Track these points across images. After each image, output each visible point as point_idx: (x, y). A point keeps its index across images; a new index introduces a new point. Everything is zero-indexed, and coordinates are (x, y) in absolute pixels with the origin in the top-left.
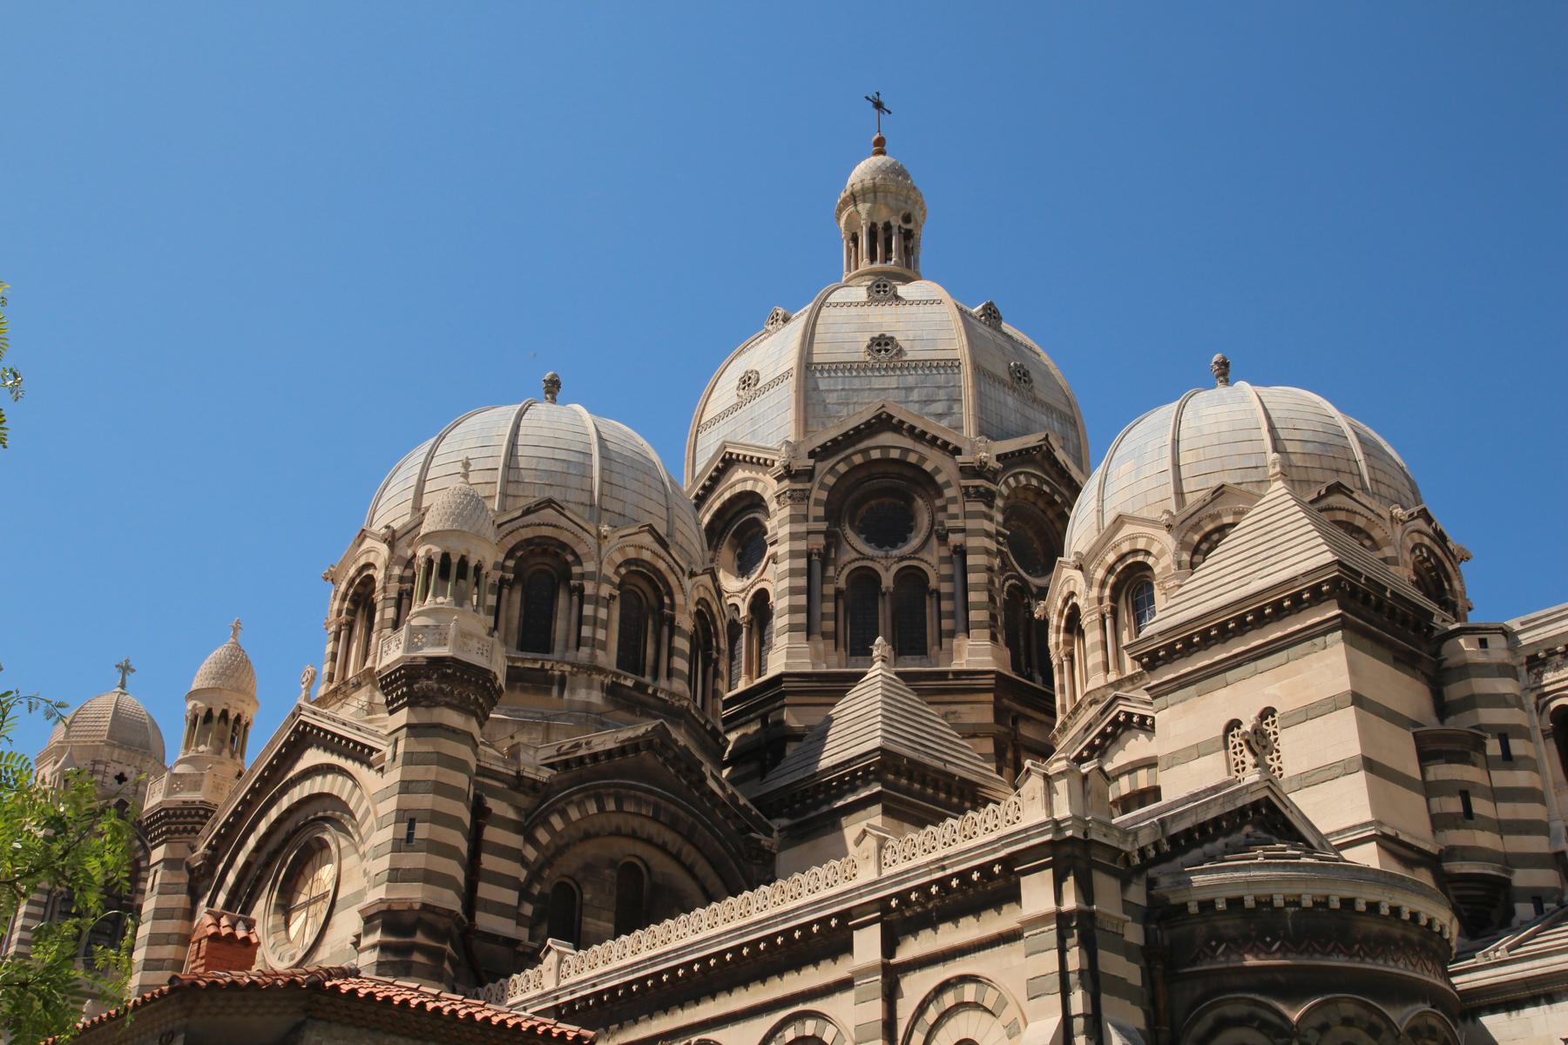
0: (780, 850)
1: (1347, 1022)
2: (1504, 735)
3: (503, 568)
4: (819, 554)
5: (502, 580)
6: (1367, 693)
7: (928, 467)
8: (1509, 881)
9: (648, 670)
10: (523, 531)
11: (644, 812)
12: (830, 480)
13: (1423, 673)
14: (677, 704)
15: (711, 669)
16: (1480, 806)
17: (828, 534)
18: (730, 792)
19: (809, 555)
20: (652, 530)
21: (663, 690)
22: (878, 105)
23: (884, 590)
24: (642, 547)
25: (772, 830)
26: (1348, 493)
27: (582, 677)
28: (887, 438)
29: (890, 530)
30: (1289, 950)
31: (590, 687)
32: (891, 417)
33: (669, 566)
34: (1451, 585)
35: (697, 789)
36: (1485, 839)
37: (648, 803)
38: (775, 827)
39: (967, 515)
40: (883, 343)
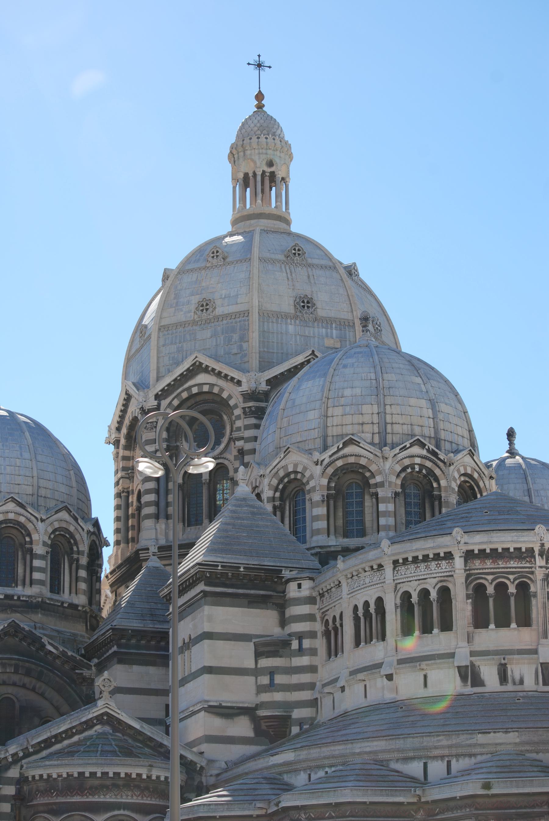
2: (300, 637)
7: (225, 395)
9: (19, 582)
11: (8, 670)
13: (273, 604)
15: (74, 566)
18: (61, 650)
20: (13, 500)
21: (23, 596)
22: (259, 66)
23: (204, 481)
24: (8, 512)
25: (91, 666)
26: (357, 444)
28: (202, 378)
30: (59, 795)
32: (201, 364)
33: (27, 518)
34: (439, 484)
36: (278, 696)
37: (11, 665)
38: (92, 664)
39: (247, 427)
40: (205, 304)
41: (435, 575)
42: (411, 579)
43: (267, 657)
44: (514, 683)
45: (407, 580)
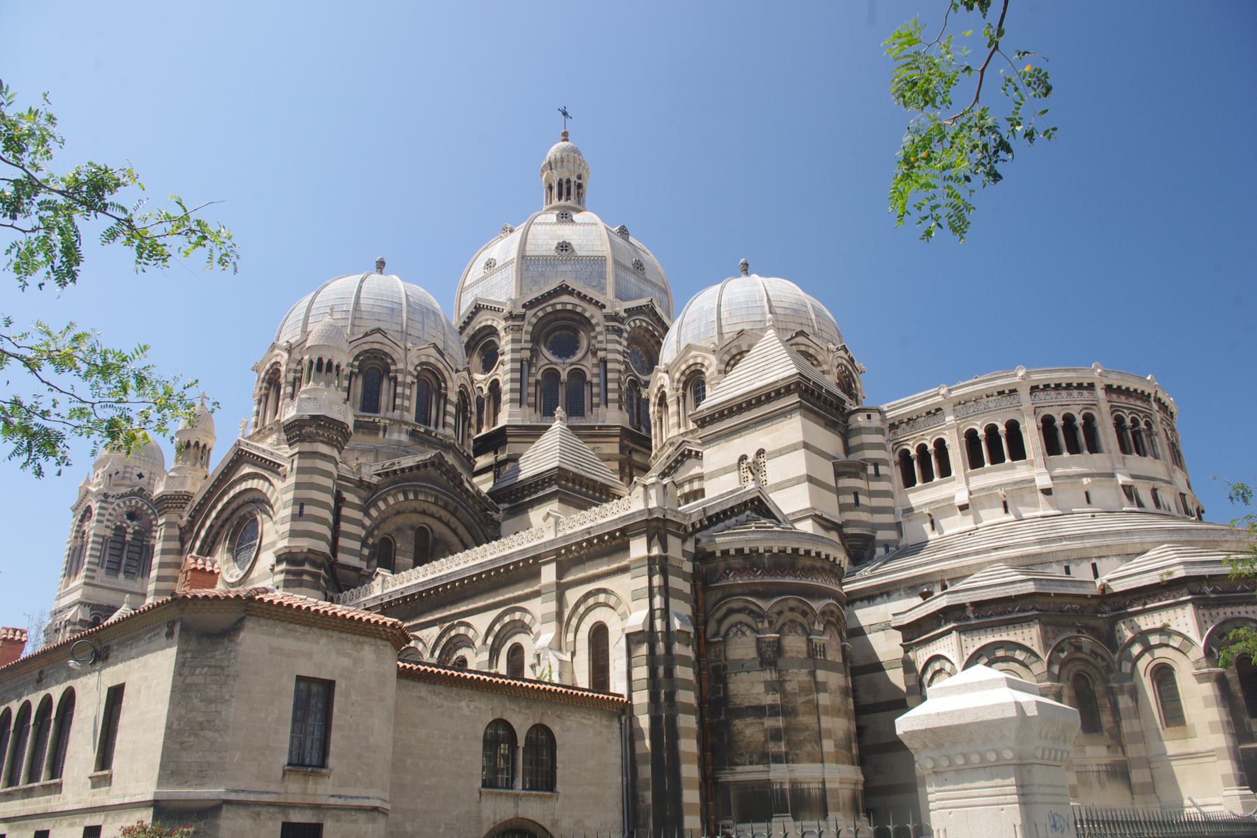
0: (503, 521)
1: (792, 609)
3: (352, 366)
4: (527, 361)
5: (352, 373)
6: (812, 442)
7: (587, 315)
8: (874, 537)
9: (432, 423)
10: (363, 345)
12: (534, 320)
14: (448, 442)
15: (467, 423)
16: (863, 500)
17: (532, 350)
19: (522, 361)
20: (435, 346)
21: (440, 434)
22: (565, 114)
25: (499, 510)
27: (396, 427)
28: (565, 298)
29: (566, 348)
30: (765, 575)
31: (400, 432)
35: (459, 488)
36: (864, 516)
37: (432, 495)
38: (501, 509)
39: (608, 341)
41: (1078, 403)
42: (1053, 404)
43: (849, 477)
44: (1165, 509)
45: (1048, 404)
